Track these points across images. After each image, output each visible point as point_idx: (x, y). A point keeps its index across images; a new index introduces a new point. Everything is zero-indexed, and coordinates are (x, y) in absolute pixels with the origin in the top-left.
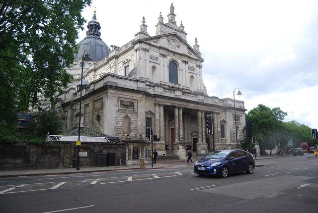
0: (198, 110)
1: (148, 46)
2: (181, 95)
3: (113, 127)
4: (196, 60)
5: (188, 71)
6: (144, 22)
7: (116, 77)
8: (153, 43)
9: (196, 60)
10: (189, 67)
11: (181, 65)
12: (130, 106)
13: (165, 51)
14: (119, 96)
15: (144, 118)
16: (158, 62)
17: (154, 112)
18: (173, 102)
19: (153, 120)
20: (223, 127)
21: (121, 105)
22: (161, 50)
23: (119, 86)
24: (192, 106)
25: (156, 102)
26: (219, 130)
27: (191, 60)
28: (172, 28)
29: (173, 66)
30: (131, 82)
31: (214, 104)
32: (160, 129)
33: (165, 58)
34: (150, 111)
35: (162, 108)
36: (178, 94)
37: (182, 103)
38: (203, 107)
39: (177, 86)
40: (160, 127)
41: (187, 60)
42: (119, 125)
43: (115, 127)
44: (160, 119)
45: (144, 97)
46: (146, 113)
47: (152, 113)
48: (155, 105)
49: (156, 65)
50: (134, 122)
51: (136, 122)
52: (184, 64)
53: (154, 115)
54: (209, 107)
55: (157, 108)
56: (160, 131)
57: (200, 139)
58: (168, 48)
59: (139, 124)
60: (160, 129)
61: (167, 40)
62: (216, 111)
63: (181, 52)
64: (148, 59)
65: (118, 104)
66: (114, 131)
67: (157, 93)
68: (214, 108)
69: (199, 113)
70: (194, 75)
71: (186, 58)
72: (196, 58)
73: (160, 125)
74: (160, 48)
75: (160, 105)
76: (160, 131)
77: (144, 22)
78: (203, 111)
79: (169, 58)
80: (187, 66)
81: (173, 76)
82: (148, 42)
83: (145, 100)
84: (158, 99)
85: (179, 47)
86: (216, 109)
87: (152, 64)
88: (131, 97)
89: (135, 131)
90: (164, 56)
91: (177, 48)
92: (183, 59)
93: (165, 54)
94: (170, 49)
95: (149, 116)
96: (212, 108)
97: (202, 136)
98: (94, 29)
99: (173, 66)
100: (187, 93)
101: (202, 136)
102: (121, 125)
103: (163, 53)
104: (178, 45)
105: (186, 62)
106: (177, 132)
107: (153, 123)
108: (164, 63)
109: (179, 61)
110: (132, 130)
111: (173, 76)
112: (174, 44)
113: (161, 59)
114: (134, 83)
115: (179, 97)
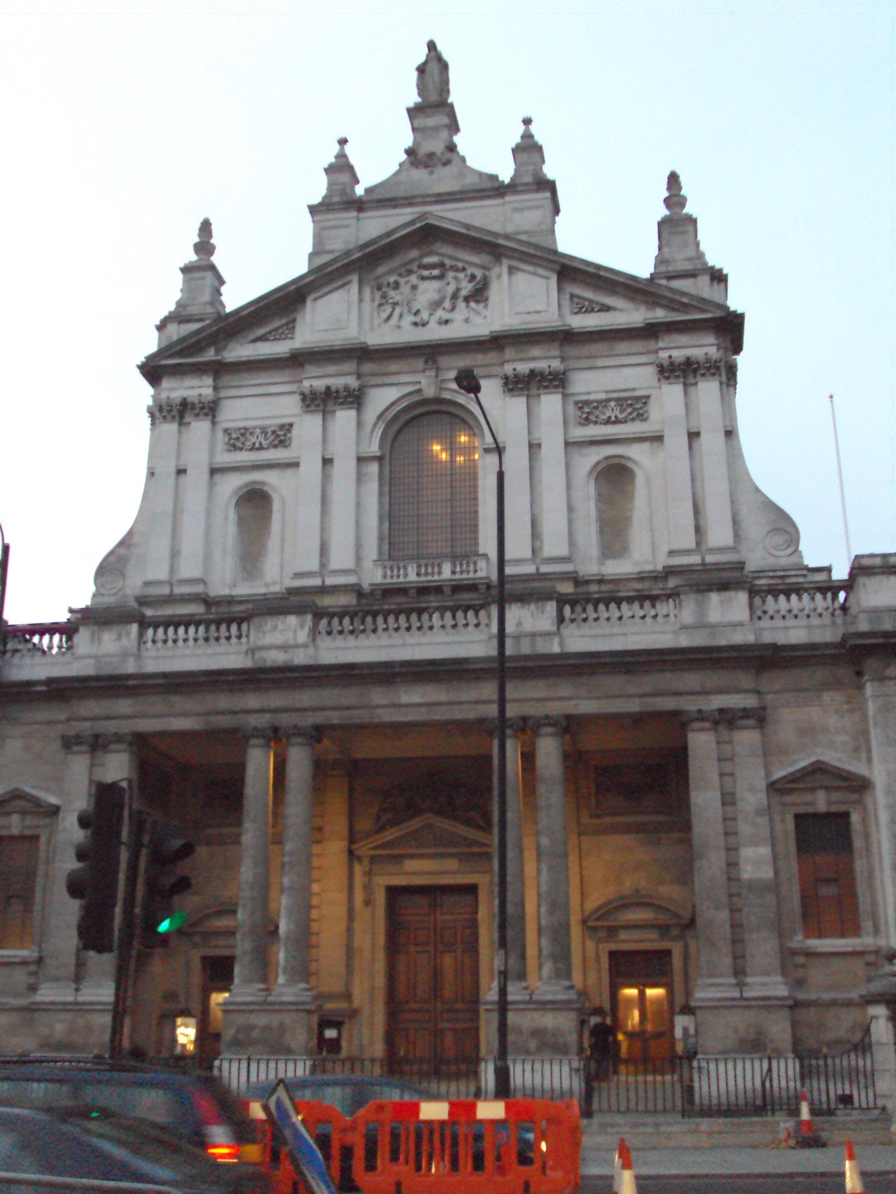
2: (302, 636)
4: (651, 331)
6: (205, 247)
9: (651, 331)
13: (349, 366)
18: (223, 701)
22: (311, 370)
28: (409, 201)
33: (345, 417)
36: (270, 638)
37: (306, 698)
41: (541, 365)
49: (270, 478)
52: (519, 404)
54: (615, 682)
68: (691, 680)
70: (634, 452)
71: (536, 351)
77: (205, 247)
78: (548, 720)
85: (479, 294)
86: (712, 679)
87: (231, 484)
92: (508, 369)
96: (648, 682)
103: (320, 384)
112: (429, 291)
115: (277, 658)
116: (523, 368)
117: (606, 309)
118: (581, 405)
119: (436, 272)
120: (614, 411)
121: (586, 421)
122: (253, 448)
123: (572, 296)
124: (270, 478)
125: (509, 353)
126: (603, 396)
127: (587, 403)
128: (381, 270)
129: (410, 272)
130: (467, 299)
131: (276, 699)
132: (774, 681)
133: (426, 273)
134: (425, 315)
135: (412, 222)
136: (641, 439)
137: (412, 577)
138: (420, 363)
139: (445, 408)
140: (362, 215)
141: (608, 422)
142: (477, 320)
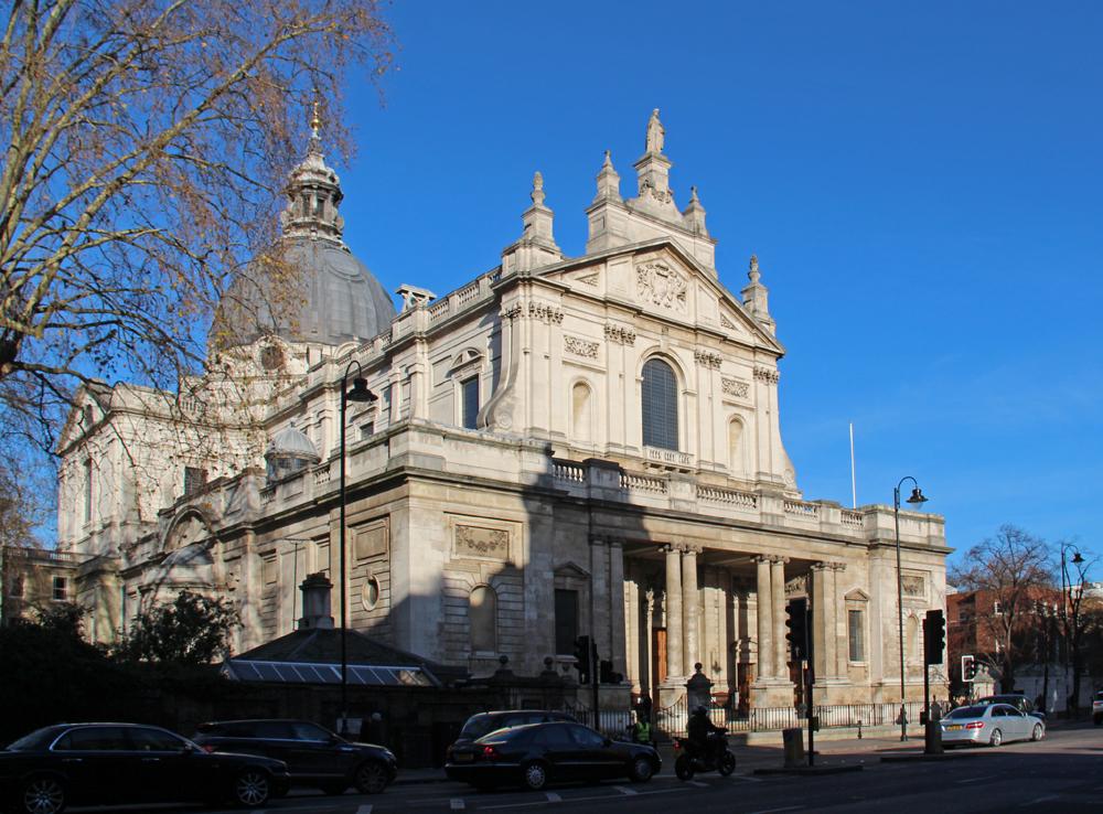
0: (758, 557)
1: (557, 297)
3: (434, 628)
4: (755, 349)
5: (720, 396)
7: (437, 432)
8: (576, 286)
9: (755, 349)
10: (724, 380)
11: (692, 376)
12: (493, 546)
13: (629, 318)
14: (452, 507)
15: (550, 591)
16: (601, 364)
17: (586, 569)
19: (583, 597)
20: (854, 619)
21: (459, 543)
22: (612, 313)
23: (449, 468)
24: (734, 541)
25: (596, 530)
26: (843, 629)
27: (732, 349)
29: (659, 386)
30: (495, 452)
31: (826, 530)
32: (611, 634)
33: (627, 347)
34: (570, 566)
35: (617, 553)
38: (778, 541)
39: (677, 460)
40: (611, 627)
41: (716, 354)
42: (454, 619)
43: (441, 625)
44: (610, 595)
45: (549, 509)
46: (557, 572)
47: (579, 571)
48: (591, 542)
49: (590, 377)
50: (512, 606)
51: (520, 606)
52: (704, 371)
53: (587, 578)
54: (802, 542)
55: (599, 552)
56: (611, 641)
57: (766, 668)
58: (638, 304)
59: (531, 614)
60: (611, 634)
61: (633, 271)
62: (832, 559)
63: (691, 322)
64: (561, 353)
65: (450, 539)
66: (436, 641)
67: (597, 494)
69: (763, 568)
70: (744, 413)
71: (711, 342)
72: (751, 340)
73: (611, 618)
74: (606, 303)
75: (609, 541)
76: (611, 641)
79: (644, 345)
80: (717, 375)
81: (660, 422)
82: (557, 280)
83: (550, 521)
84: (600, 518)
85: (682, 296)
87: (573, 374)
88: (496, 513)
89: (516, 640)
90: (626, 338)
91: (675, 303)
92: (701, 349)
93: (629, 329)
94: (648, 308)
95: (569, 583)
97: (775, 654)
98: (314, 204)
99: (659, 386)
100: (717, 490)
101: (775, 654)
102: (461, 620)
103: (619, 326)
104: (678, 291)
105: (714, 362)
106: (675, 641)
107: (583, 610)
108: (627, 363)
109: (686, 358)
110: (506, 639)
111: (660, 422)
112: (660, 285)
113: (611, 355)
114: (509, 454)
115: (684, 507)
116: (708, 352)
117: (733, 328)
118: (724, 380)
119: (665, 273)
120: (734, 388)
121: (725, 390)
122: (579, 354)
123: (722, 315)
124: (590, 377)
125: (700, 338)
126: (732, 378)
127: (726, 380)
128: (641, 258)
129: (652, 267)
130: (679, 296)
131: (684, 528)
132: (848, 550)
133: (661, 272)
134: (658, 299)
135: (663, 239)
136: (747, 408)
137: (663, 459)
138: (659, 328)
139: (664, 359)
140: (631, 217)
141: (733, 394)
142: (681, 311)
